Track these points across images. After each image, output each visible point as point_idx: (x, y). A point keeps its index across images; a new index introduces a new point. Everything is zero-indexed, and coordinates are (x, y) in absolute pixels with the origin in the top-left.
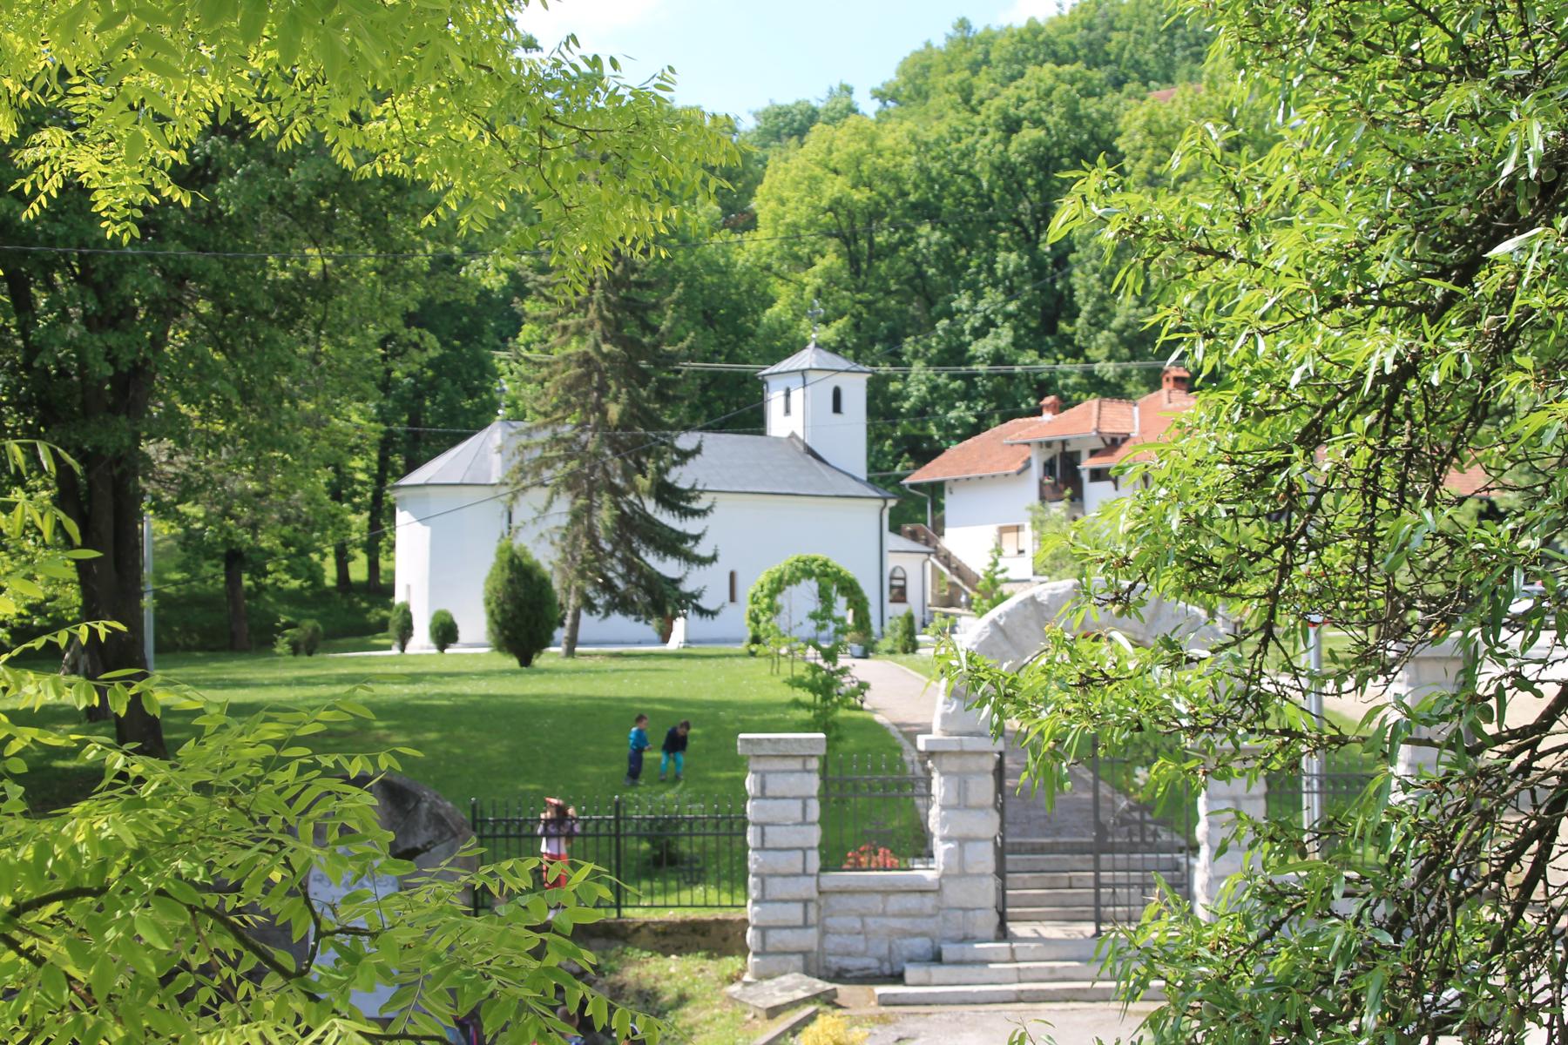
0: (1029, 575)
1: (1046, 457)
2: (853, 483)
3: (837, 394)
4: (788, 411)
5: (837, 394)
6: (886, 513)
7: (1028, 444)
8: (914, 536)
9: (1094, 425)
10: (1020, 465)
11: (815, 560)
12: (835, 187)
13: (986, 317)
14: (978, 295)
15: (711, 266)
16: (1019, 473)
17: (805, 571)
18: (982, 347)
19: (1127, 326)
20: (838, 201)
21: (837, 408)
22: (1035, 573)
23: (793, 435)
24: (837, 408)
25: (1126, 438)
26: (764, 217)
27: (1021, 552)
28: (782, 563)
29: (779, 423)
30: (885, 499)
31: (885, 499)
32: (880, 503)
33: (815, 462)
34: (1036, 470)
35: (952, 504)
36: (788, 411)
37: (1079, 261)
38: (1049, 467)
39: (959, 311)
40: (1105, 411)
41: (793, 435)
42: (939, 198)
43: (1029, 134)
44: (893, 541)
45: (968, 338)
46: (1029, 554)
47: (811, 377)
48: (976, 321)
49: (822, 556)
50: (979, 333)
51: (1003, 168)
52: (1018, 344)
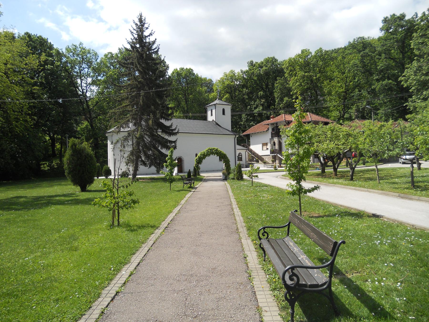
0: (269, 154)
1: (272, 127)
2: (228, 132)
3: (224, 110)
4: (212, 115)
5: (224, 110)
6: (236, 138)
7: (268, 125)
8: (243, 146)
9: (284, 119)
10: (267, 129)
11: (214, 149)
12: (227, 83)
13: (257, 105)
14: (255, 101)
15: (204, 99)
16: (267, 131)
17: (211, 152)
18: (256, 111)
19: (286, 103)
20: (228, 85)
21: (224, 113)
22: (271, 154)
23: (213, 120)
24: (224, 113)
25: (291, 121)
26: (215, 89)
27: (268, 149)
28: (205, 150)
29: (210, 118)
30: (236, 135)
31: (236, 135)
32: (234, 136)
33: (218, 126)
34: (270, 130)
35: (252, 140)
36: (212, 115)
37: (276, 91)
38: (273, 130)
39: (252, 104)
40: (286, 116)
41: (213, 120)
42: (247, 83)
43: (264, 68)
44: (238, 147)
45: (253, 109)
46: (269, 149)
47: (217, 105)
48: (255, 106)
49: (216, 148)
50: (255, 108)
51: (259, 76)
52: (263, 110)
